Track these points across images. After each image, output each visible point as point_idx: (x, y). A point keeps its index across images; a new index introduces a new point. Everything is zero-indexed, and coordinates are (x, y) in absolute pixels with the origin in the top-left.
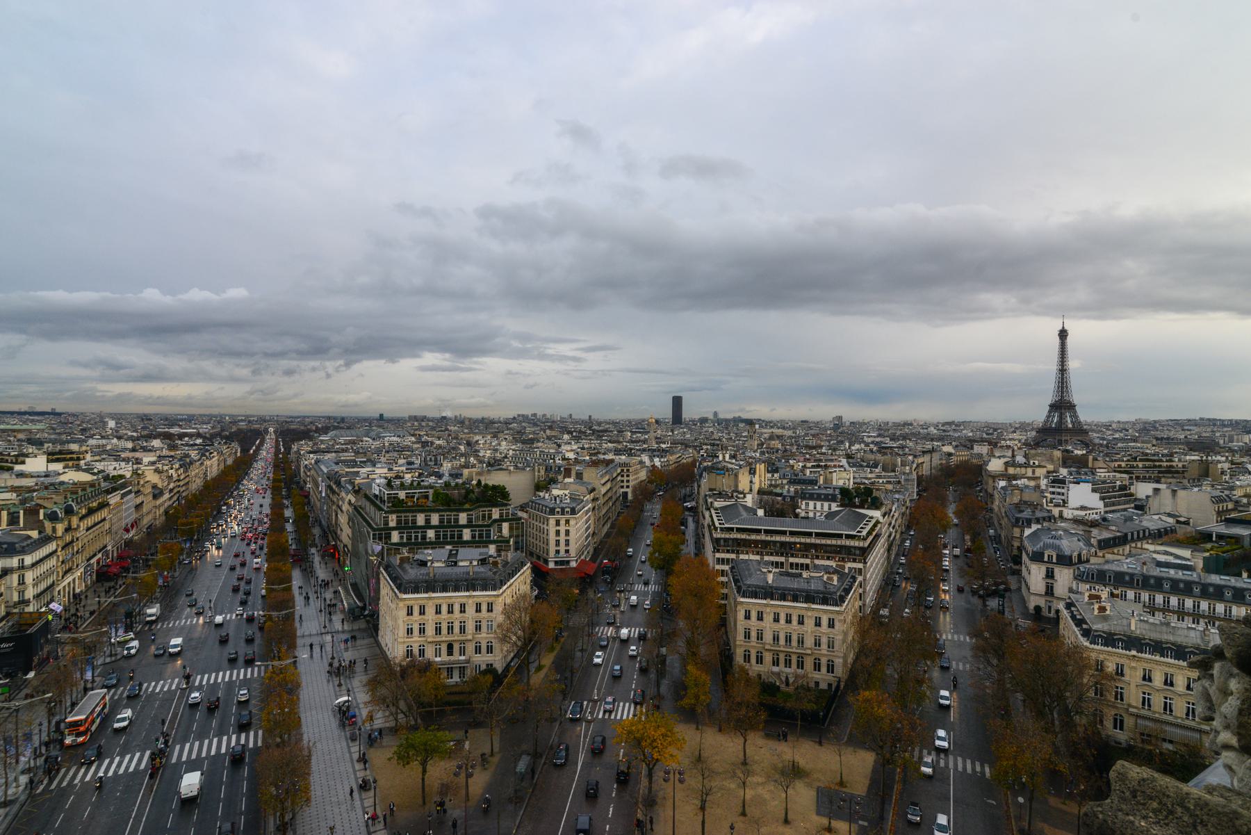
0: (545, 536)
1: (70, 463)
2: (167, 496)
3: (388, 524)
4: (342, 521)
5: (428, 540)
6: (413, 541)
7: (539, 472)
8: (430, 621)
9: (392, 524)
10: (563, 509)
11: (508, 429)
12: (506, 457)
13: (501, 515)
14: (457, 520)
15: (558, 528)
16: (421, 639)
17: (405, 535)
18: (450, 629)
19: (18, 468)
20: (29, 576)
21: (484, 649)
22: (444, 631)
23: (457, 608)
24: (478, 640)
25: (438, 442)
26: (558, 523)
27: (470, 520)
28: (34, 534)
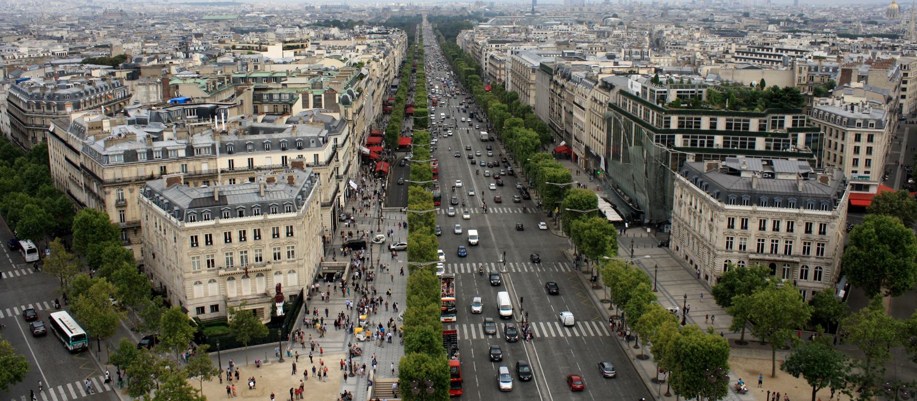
0: (838, 152)
1: (298, 50)
2: (382, 85)
3: (669, 126)
4: (584, 120)
5: (715, 147)
6: (698, 146)
7: (800, 72)
8: (753, 237)
9: (674, 125)
10: (866, 121)
11: (691, 16)
12: (727, 52)
13: (794, 123)
14: (746, 126)
15: (857, 144)
16: (742, 254)
17: (689, 140)
18: (774, 248)
19: (264, 54)
20: (341, 153)
21: (811, 273)
22: (767, 249)
23: (783, 226)
24: (806, 264)
25: (616, 32)
26: (858, 138)
27: (762, 128)
28: (337, 116)
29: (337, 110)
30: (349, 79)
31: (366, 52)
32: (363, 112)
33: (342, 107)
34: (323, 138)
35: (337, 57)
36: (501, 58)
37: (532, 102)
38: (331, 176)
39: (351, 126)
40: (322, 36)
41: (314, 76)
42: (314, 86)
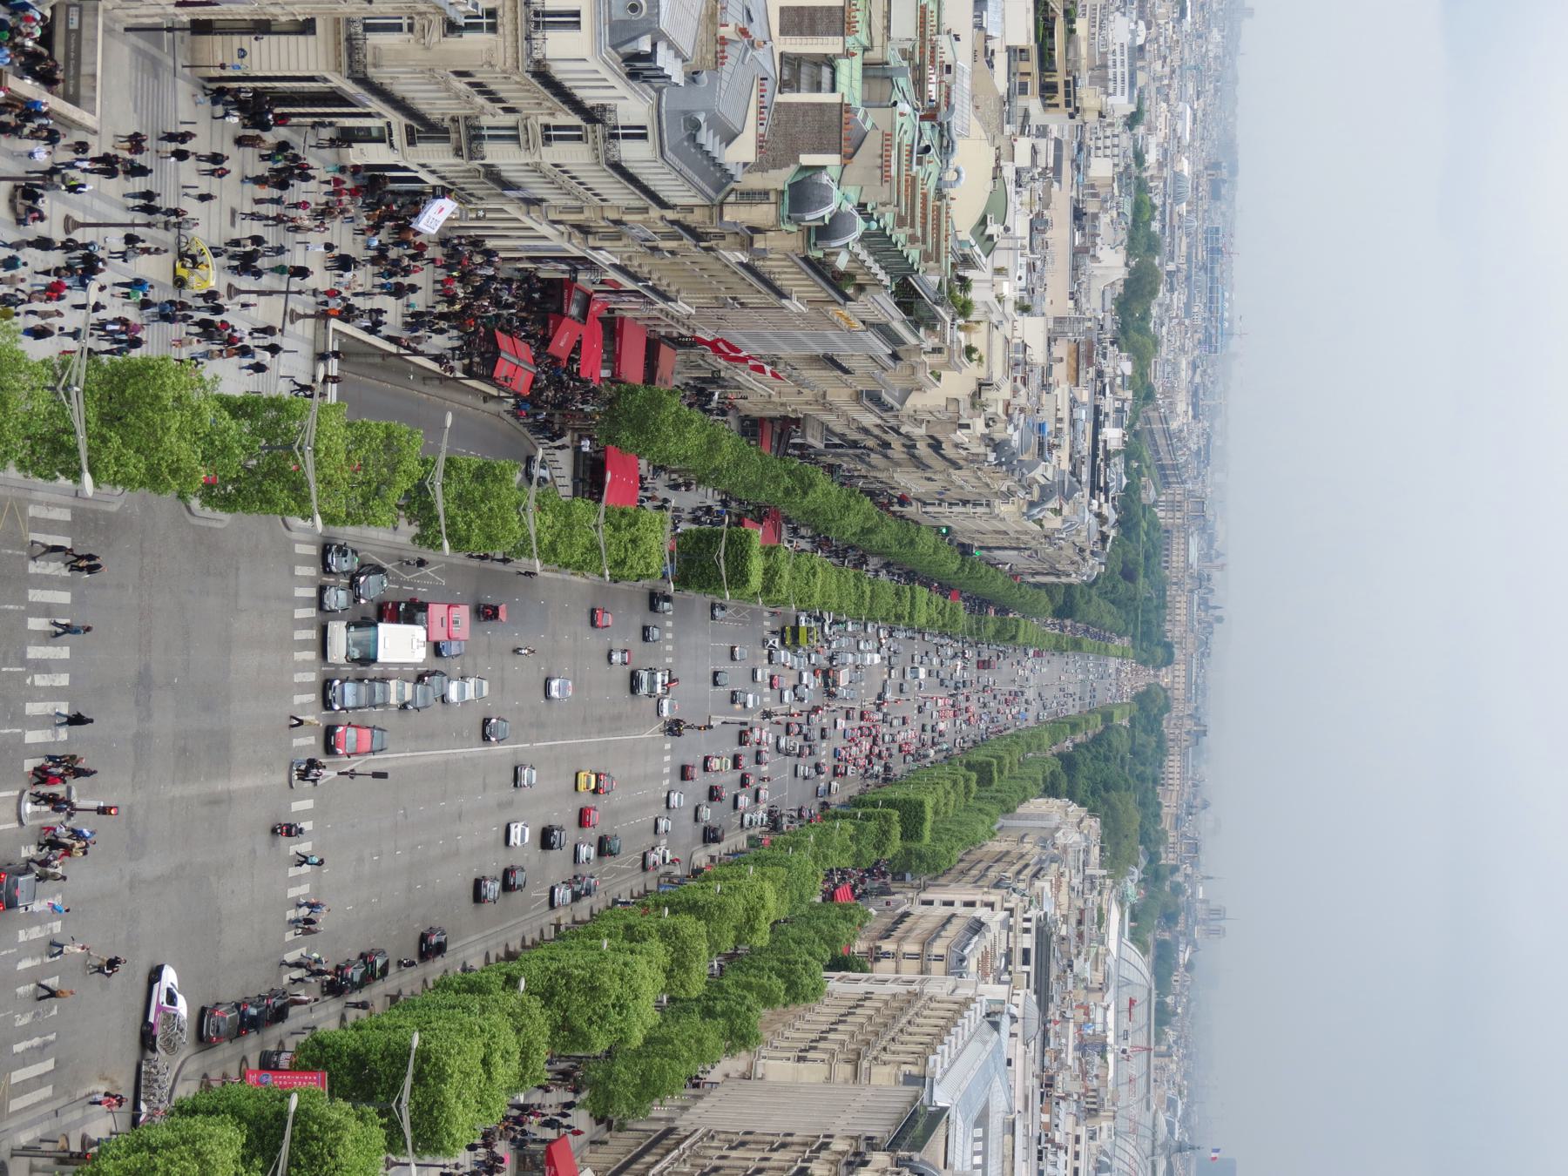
1: (1032, 66)
2: (869, 420)
29: (769, 156)
30: (900, 236)
31: (1019, 365)
32: (757, 296)
33: (780, 179)
34: (650, 57)
35: (996, 207)
36: (972, 964)
37: (776, 1068)
38: (481, 89)
39: (692, 219)
40: (1091, 207)
41: (920, 82)
42: (875, 72)
